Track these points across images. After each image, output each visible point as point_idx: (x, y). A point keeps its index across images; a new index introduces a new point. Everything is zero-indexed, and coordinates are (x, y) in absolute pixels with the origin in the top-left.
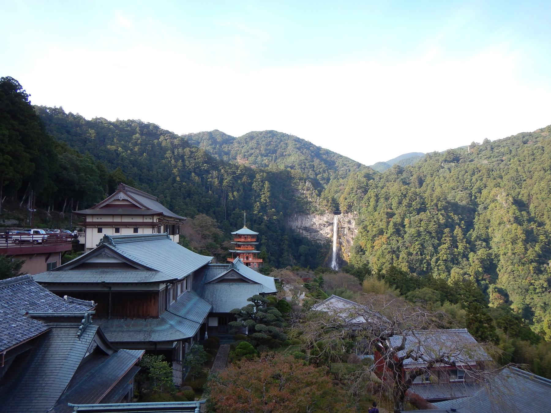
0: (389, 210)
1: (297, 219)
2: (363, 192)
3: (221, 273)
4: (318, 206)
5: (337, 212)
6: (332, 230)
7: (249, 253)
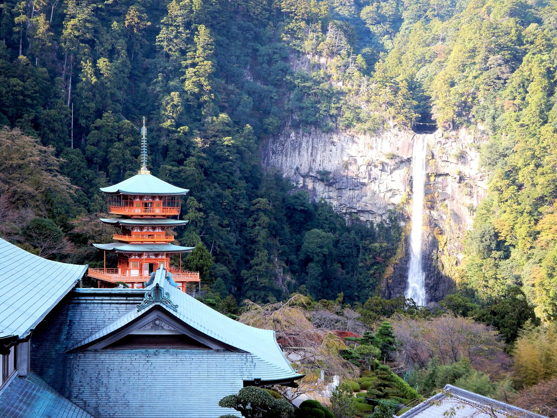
1: (296, 147)
2: (507, 62)
3: (120, 317)
4: (363, 105)
5: (424, 124)
7: (157, 254)
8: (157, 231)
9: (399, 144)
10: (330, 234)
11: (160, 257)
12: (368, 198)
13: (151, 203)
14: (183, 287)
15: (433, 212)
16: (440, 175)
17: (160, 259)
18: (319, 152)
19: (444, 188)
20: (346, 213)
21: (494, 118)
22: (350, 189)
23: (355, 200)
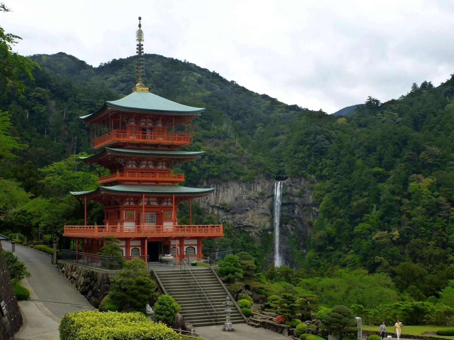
0: (377, 169)
6: (272, 209)
7: (161, 198)
8: (160, 167)
9: (266, 187)
10: (229, 240)
11: (165, 204)
12: (250, 218)
13: (151, 129)
14: (198, 245)
15: (287, 226)
16: (291, 204)
17: (165, 207)
18: (221, 193)
19: (293, 212)
20: (237, 228)
21: (321, 170)
22: (239, 214)
23: (242, 220)
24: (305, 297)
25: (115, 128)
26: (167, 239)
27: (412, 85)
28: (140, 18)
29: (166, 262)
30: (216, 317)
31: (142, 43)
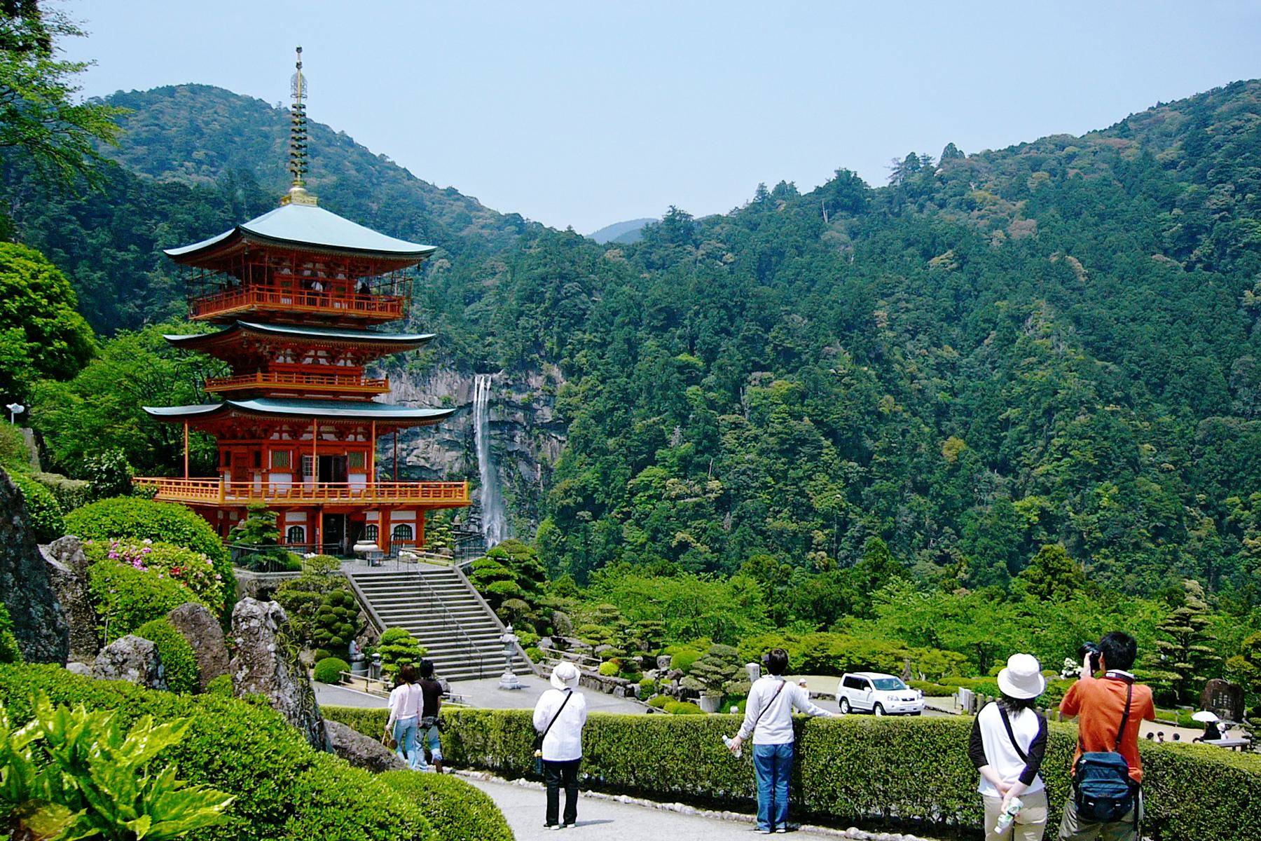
0: (684, 357)
17: (350, 445)
19: (512, 439)
21: (572, 356)
24: (645, 626)
25: (254, 283)
26: (359, 510)
27: (756, 187)
28: (299, 50)
29: (362, 555)
30: (482, 664)
31: (303, 102)
